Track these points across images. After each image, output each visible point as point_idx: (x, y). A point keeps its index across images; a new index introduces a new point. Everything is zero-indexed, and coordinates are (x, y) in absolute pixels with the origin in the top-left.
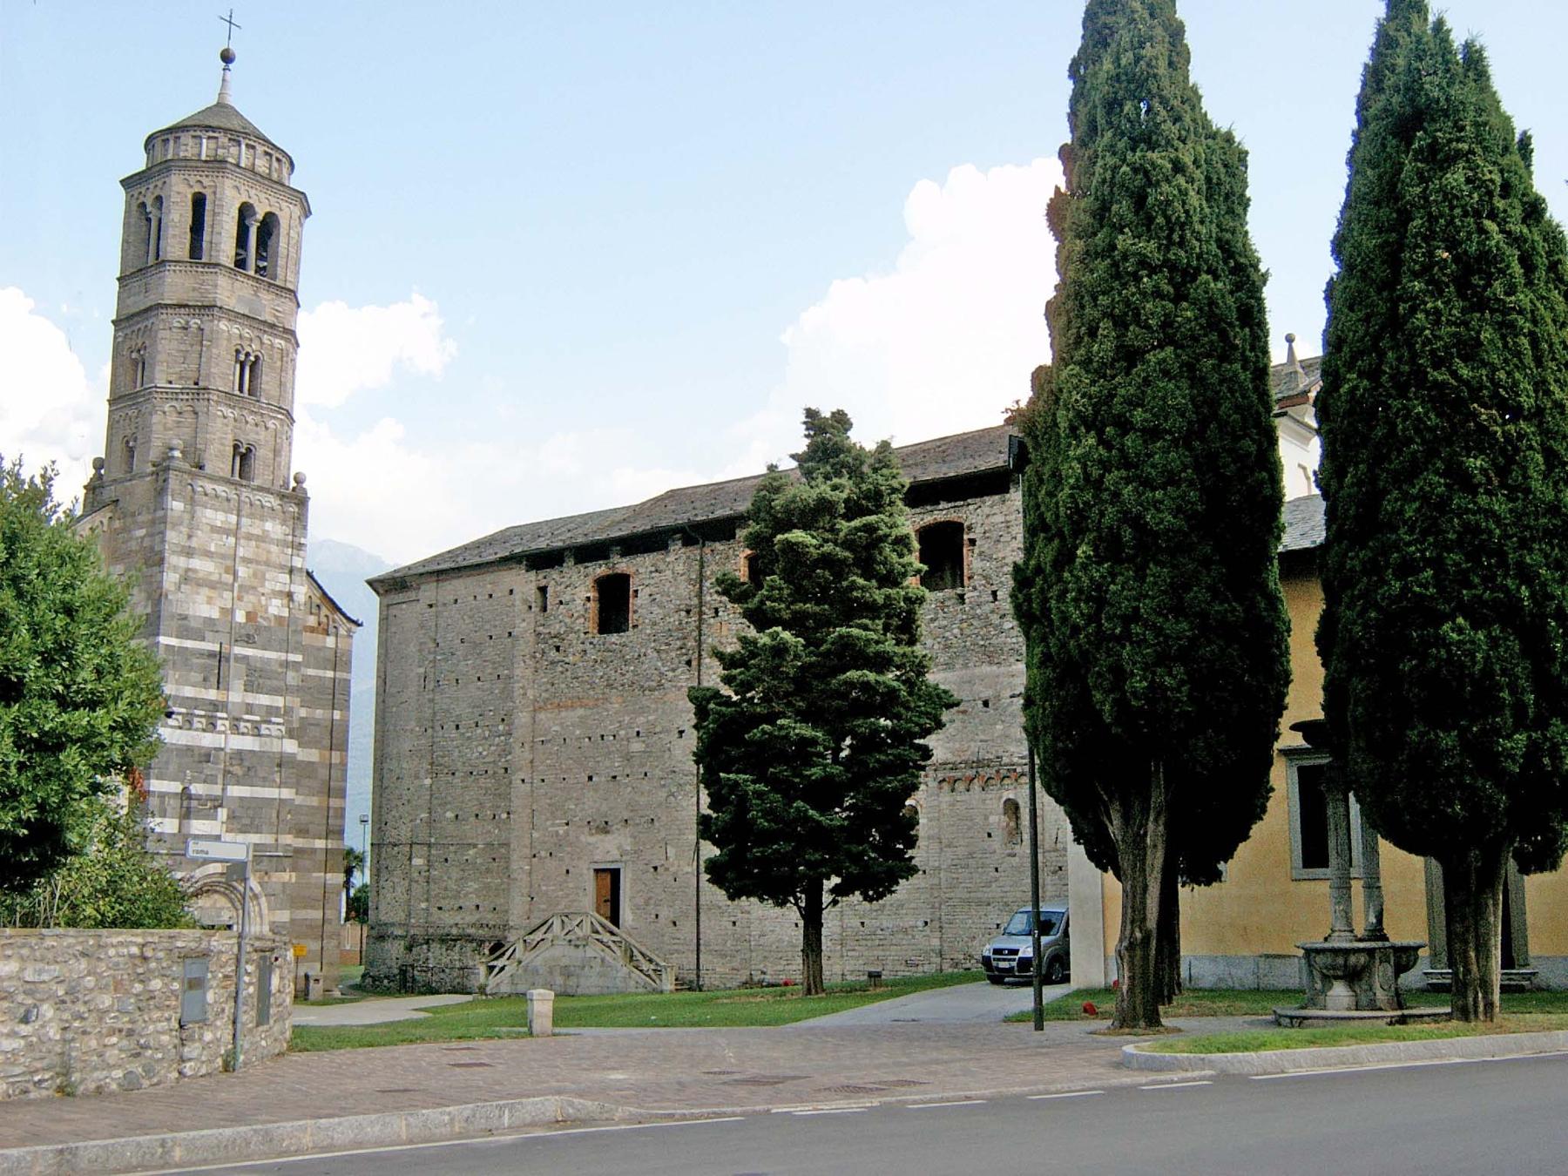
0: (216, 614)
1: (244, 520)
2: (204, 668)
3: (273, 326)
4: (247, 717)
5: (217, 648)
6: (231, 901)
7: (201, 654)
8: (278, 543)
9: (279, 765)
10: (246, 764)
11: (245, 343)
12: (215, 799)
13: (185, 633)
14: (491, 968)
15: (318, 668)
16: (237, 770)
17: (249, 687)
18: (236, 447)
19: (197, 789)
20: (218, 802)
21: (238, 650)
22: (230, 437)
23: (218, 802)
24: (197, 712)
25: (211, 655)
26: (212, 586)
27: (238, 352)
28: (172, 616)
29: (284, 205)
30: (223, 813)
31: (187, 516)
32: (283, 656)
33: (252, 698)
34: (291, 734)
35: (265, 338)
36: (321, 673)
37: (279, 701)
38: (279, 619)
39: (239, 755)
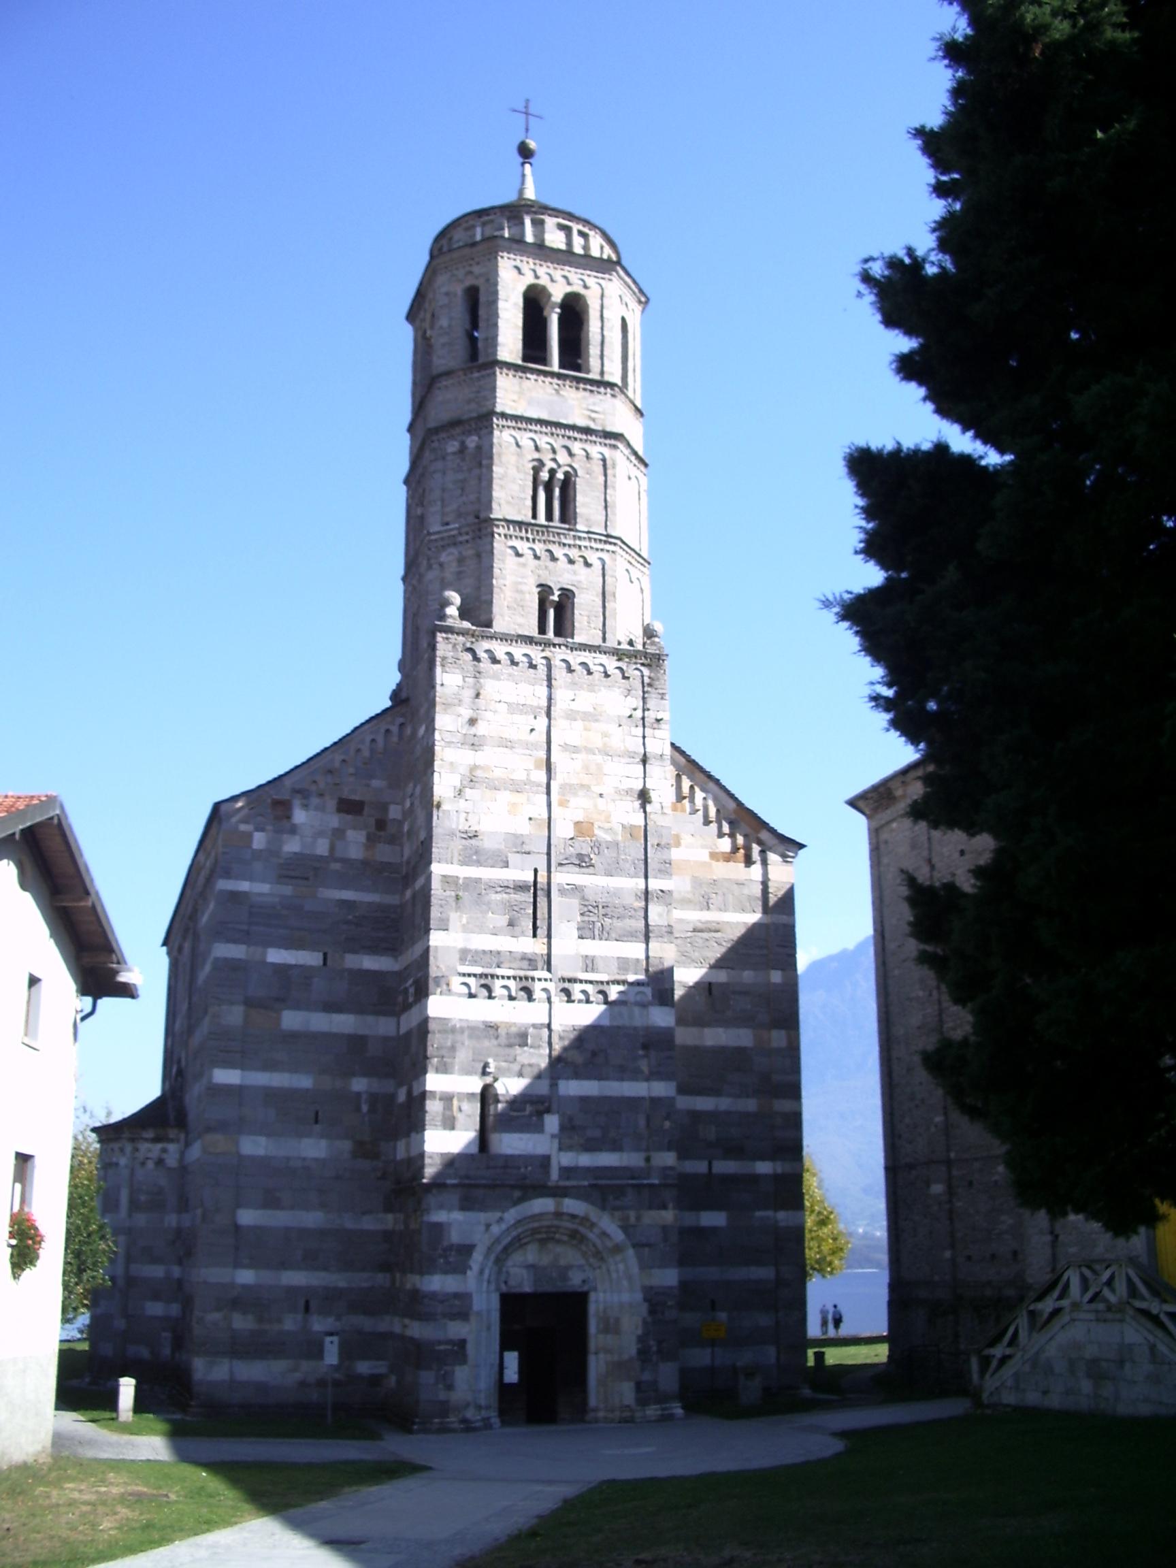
0: (523, 828)
3: (587, 431)
6: (584, 1254)
9: (645, 1047)
11: (547, 458)
13: (474, 856)
14: (985, 1362)
17: (586, 932)
24: (499, 972)
25: (520, 887)
26: (517, 787)
27: (536, 471)
28: (452, 834)
29: (591, 282)
30: (552, 1122)
31: (468, 694)
35: (576, 447)
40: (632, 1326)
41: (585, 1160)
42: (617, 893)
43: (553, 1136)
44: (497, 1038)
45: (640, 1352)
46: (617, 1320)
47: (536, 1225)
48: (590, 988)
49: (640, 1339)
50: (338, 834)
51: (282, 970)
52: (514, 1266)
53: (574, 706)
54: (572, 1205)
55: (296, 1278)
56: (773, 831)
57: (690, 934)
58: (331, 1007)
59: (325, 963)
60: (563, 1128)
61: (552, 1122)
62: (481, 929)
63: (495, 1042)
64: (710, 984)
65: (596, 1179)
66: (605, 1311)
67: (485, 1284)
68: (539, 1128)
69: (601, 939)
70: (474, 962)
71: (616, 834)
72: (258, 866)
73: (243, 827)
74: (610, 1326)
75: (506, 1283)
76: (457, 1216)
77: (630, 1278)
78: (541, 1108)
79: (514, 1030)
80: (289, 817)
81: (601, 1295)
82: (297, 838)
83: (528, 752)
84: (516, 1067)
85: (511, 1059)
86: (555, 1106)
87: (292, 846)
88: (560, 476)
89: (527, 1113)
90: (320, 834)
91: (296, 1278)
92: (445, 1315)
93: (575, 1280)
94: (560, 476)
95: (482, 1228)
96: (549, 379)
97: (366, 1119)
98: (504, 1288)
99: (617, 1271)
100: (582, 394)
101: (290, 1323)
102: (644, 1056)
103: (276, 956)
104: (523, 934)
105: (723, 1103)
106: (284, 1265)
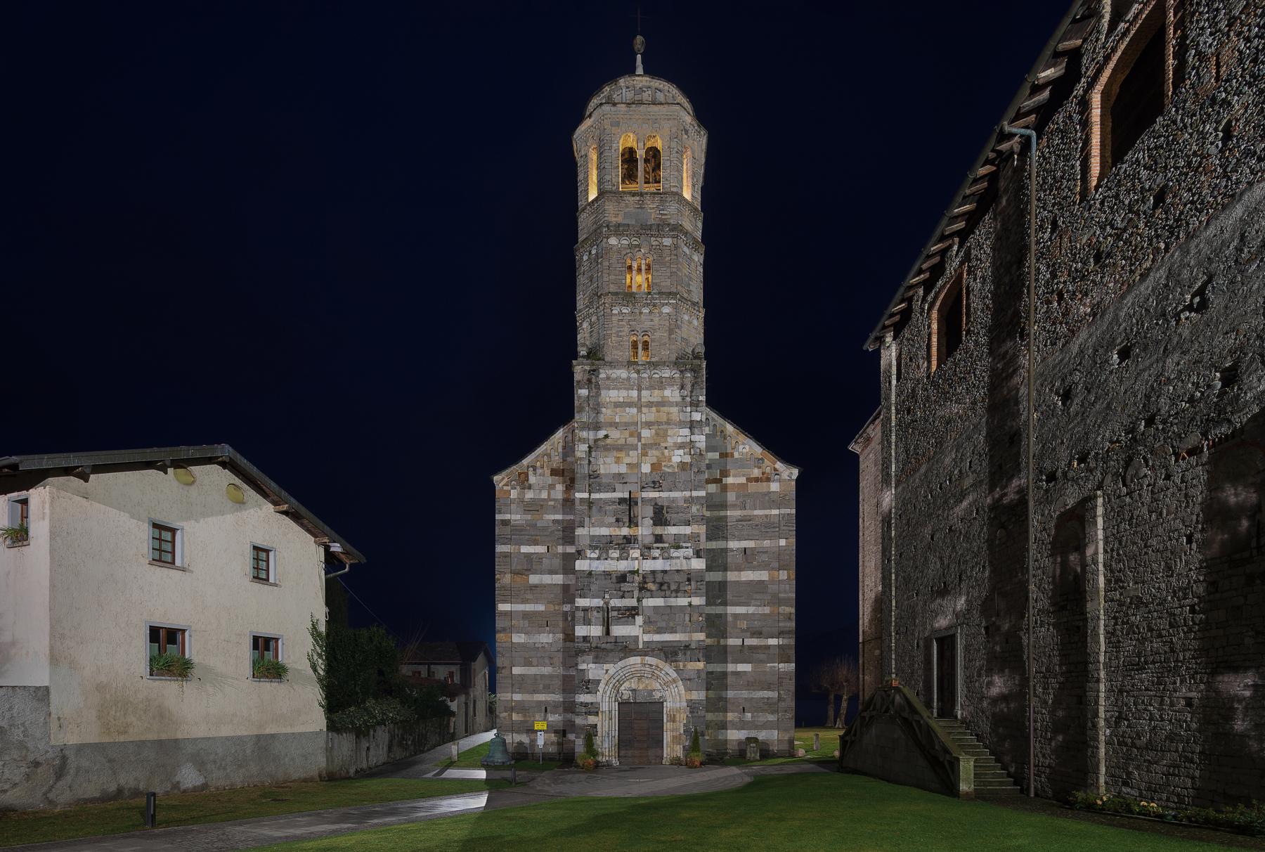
1: (644, 393)
5: (626, 495)
8: (677, 404)
12: (634, 608)
16: (651, 586)
19: (615, 602)
21: (644, 495)
25: (621, 501)
26: (619, 448)
32: (687, 494)
33: (659, 530)
34: (698, 554)
38: (683, 466)
41: (657, 638)
54: (649, 660)
60: (645, 622)
62: (602, 525)
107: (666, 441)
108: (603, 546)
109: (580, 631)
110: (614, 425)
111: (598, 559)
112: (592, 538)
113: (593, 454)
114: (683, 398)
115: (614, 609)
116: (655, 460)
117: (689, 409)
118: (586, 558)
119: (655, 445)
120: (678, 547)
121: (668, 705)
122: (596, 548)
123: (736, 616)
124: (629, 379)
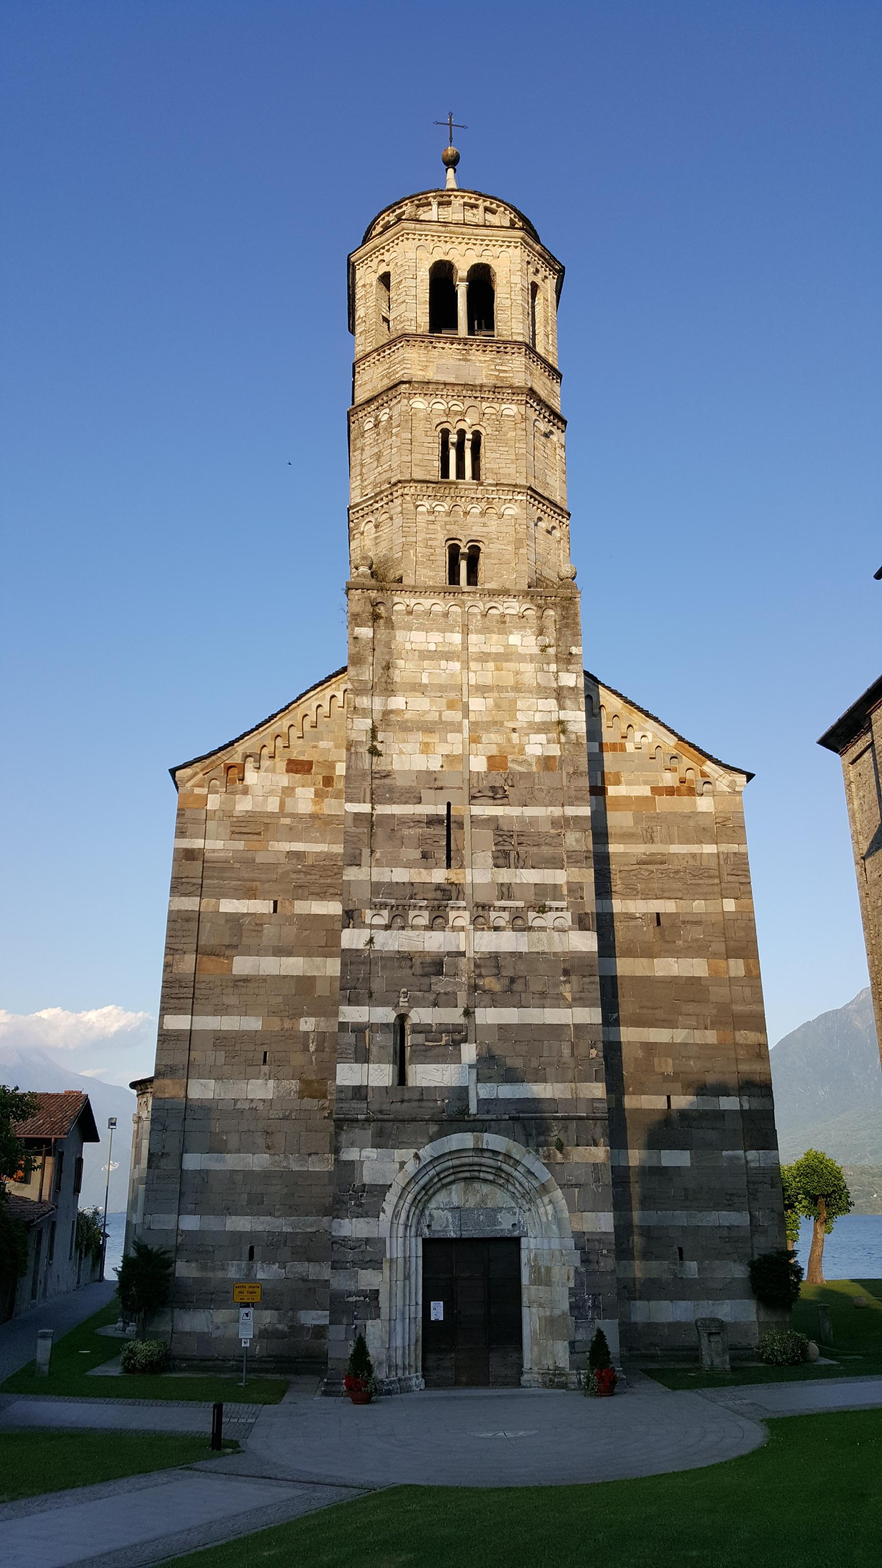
0: (435, 764)
1: (473, 638)
2: (422, 841)
3: (495, 389)
4: (498, 903)
5: (442, 810)
7: (416, 821)
8: (532, 658)
9: (566, 973)
10: (508, 972)
12: (455, 1029)
15: (688, 842)
17: (502, 859)
18: (454, 553)
19: (420, 1015)
20: (458, 1036)
21: (477, 810)
22: (441, 537)
23: (458, 1036)
25: (432, 821)
26: (428, 728)
27: (445, 433)
28: (363, 775)
30: (469, 1052)
32: (557, 811)
33: (505, 876)
36: (694, 848)
37: (559, 877)
38: (547, 762)
39: (494, 961)
40: (564, 1274)
41: (506, 1091)
42: (534, 820)
43: (471, 1066)
44: (411, 967)
45: (572, 1307)
46: (548, 1269)
47: (456, 1162)
48: (506, 915)
49: (572, 1292)
50: (288, 791)
51: (235, 919)
52: (437, 1208)
53: (486, 649)
54: (494, 1141)
55: (241, 1224)
56: (717, 762)
57: (634, 867)
58: (280, 951)
59: (275, 911)
60: (480, 1059)
61: (469, 1052)
62: (395, 862)
63: (410, 972)
64: (658, 914)
65: (518, 1113)
66: (536, 1255)
67: (401, 1228)
68: (457, 1059)
69: (517, 868)
70: (389, 895)
71: (530, 765)
72: (211, 825)
73: (197, 791)
74: (543, 1278)
75: (429, 1226)
76: (371, 1153)
77: (559, 1221)
78: (457, 1037)
79: (428, 959)
80: (242, 779)
81: (532, 1240)
82: (249, 796)
83: (439, 694)
84: (432, 997)
85: (425, 988)
86: (471, 1037)
87: (244, 805)
88: (469, 436)
89: (443, 1043)
90: (271, 793)
91: (241, 1224)
92: (354, 1264)
93: (505, 1225)
94: (469, 436)
95: (398, 1166)
96: (455, 346)
97: (314, 1058)
98: (427, 1233)
99: (546, 1214)
100: (489, 356)
101: (233, 1272)
102: (565, 982)
103: (228, 906)
104: (437, 865)
105: (680, 1035)
106: (229, 1211)
107: (514, 718)
108: (398, 904)
109: (348, 1075)
110: (419, 688)
111: (387, 927)
112: (376, 887)
113: (380, 736)
114: (544, 649)
115: (419, 1029)
116: (494, 750)
117: (553, 667)
118: (362, 925)
119: (495, 725)
120: (542, 909)
121: (529, 1247)
122: (384, 906)
123: (650, 1048)
124: (446, 615)
